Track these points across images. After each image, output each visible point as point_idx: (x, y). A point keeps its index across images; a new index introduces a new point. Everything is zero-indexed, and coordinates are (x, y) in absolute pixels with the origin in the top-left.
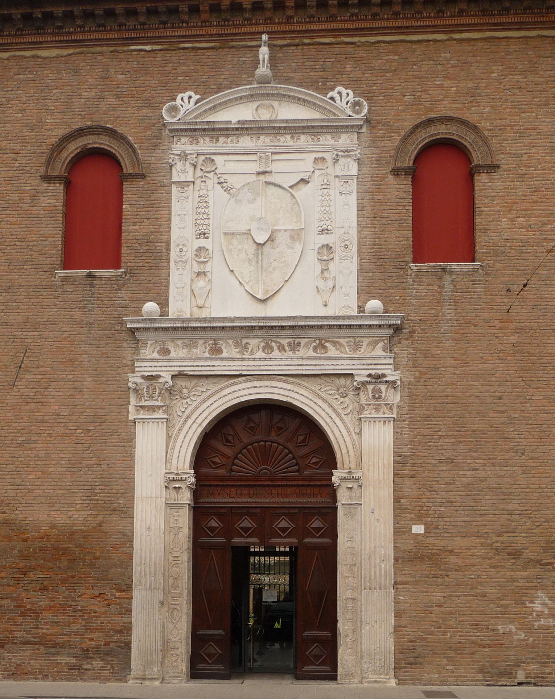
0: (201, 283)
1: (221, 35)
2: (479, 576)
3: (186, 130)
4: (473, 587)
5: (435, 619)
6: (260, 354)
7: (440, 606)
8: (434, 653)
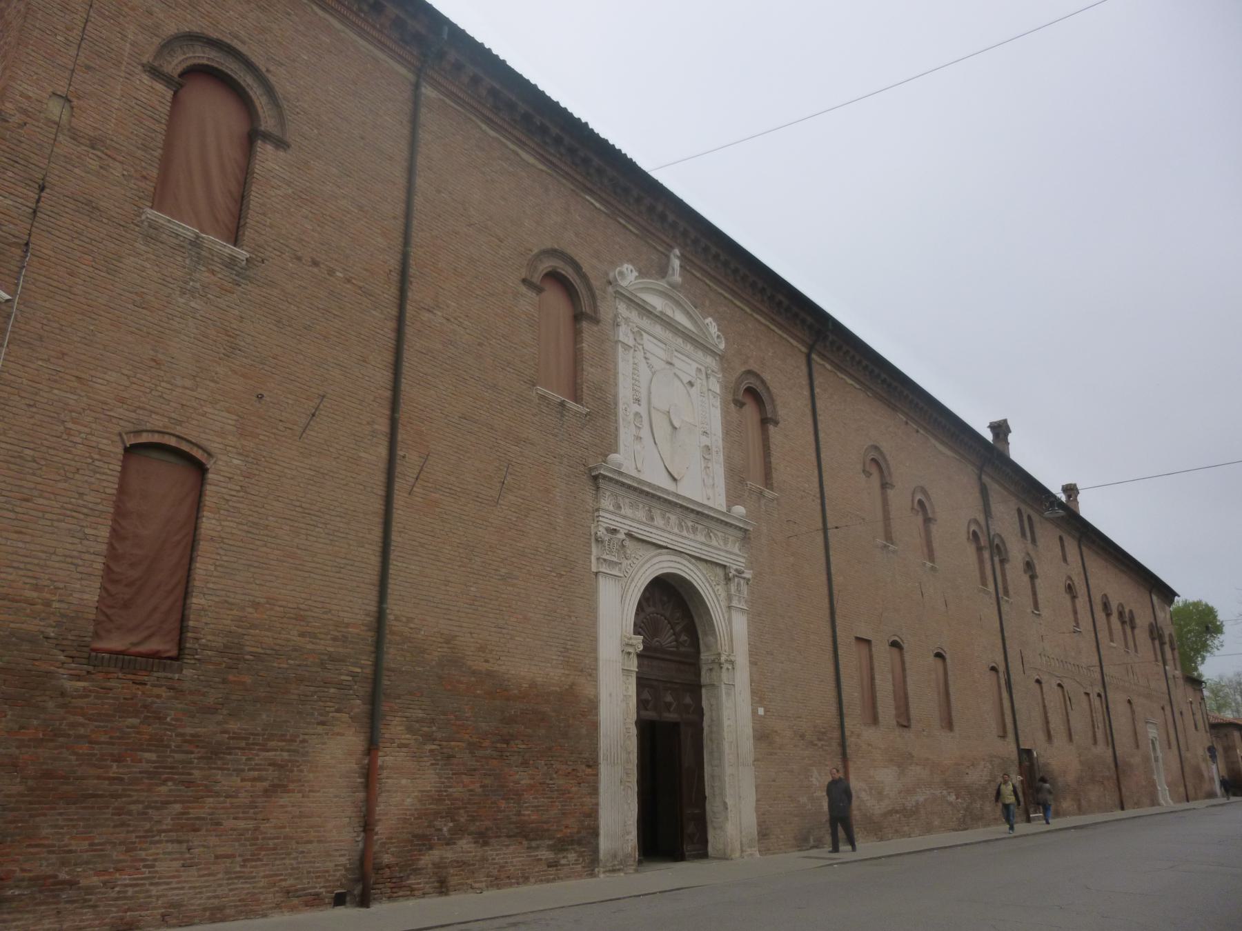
6: (676, 530)
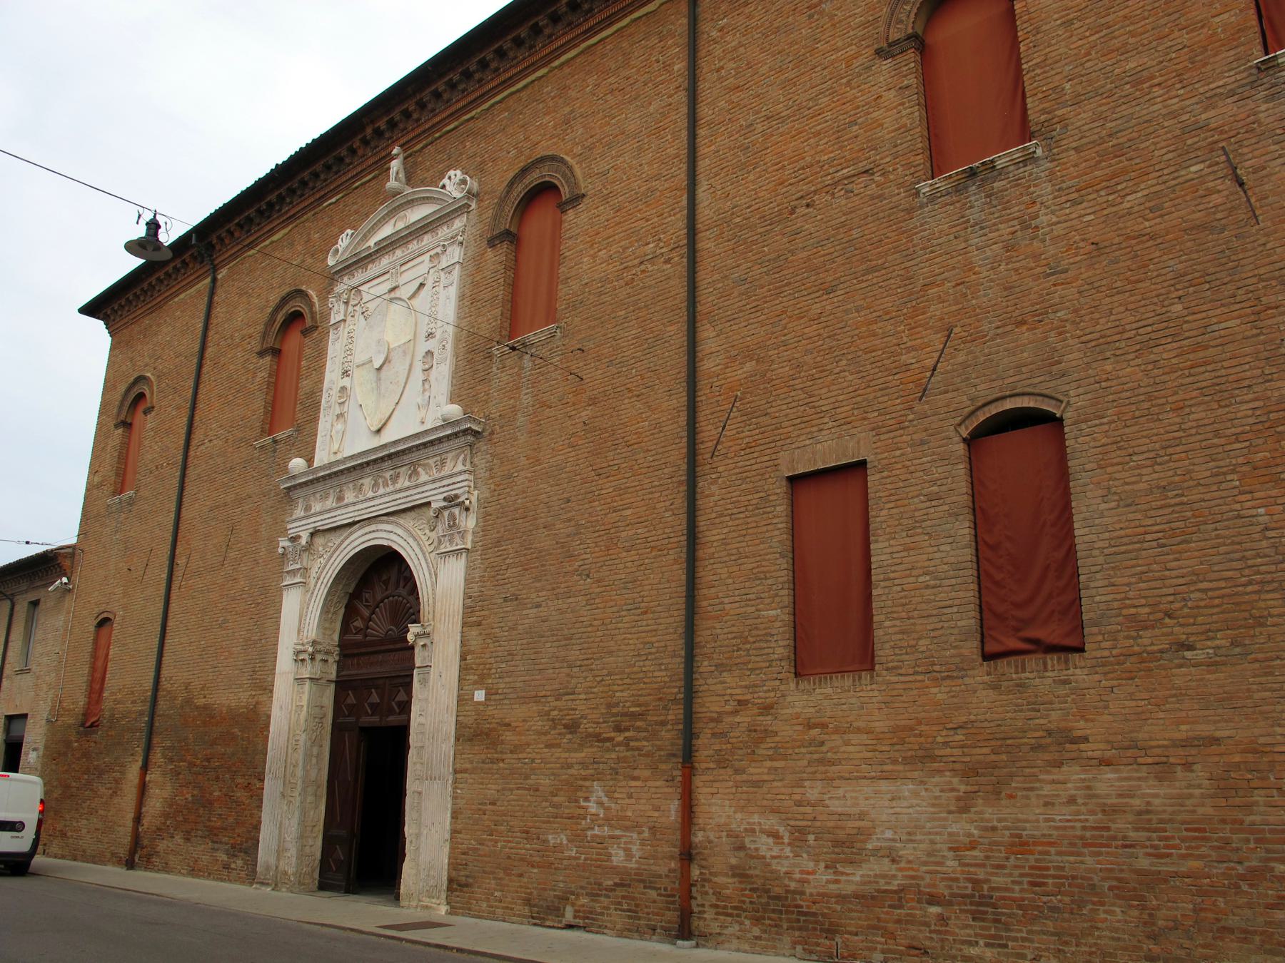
0: (339, 427)
1: (376, 162)
2: (533, 760)
3: (344, 269)
4: (527, 777)
5: (487, 823)
7: (493, 804)
8: (484, 872)
